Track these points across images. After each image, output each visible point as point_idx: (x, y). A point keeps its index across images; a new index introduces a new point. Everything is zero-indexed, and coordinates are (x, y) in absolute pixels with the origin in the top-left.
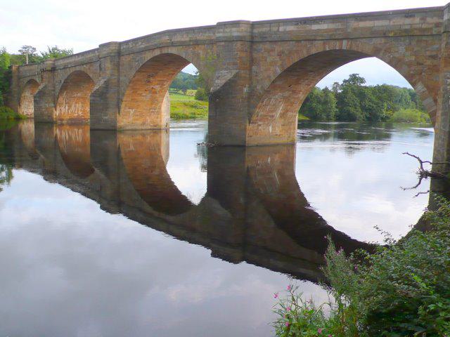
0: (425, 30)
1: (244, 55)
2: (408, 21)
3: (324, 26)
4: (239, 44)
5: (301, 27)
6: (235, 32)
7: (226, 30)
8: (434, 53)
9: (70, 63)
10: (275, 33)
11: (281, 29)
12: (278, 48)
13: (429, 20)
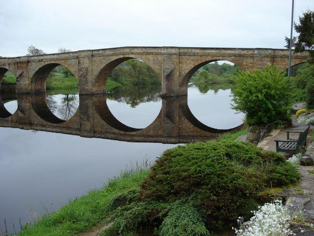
1: (177, 60)
2: (243, 52)
3: (213, 51)
4: (175, 56)
6: (173, 51)
9: (47, 59)
10: (190, 52)
11: (193, 51)
12: (191, 58)
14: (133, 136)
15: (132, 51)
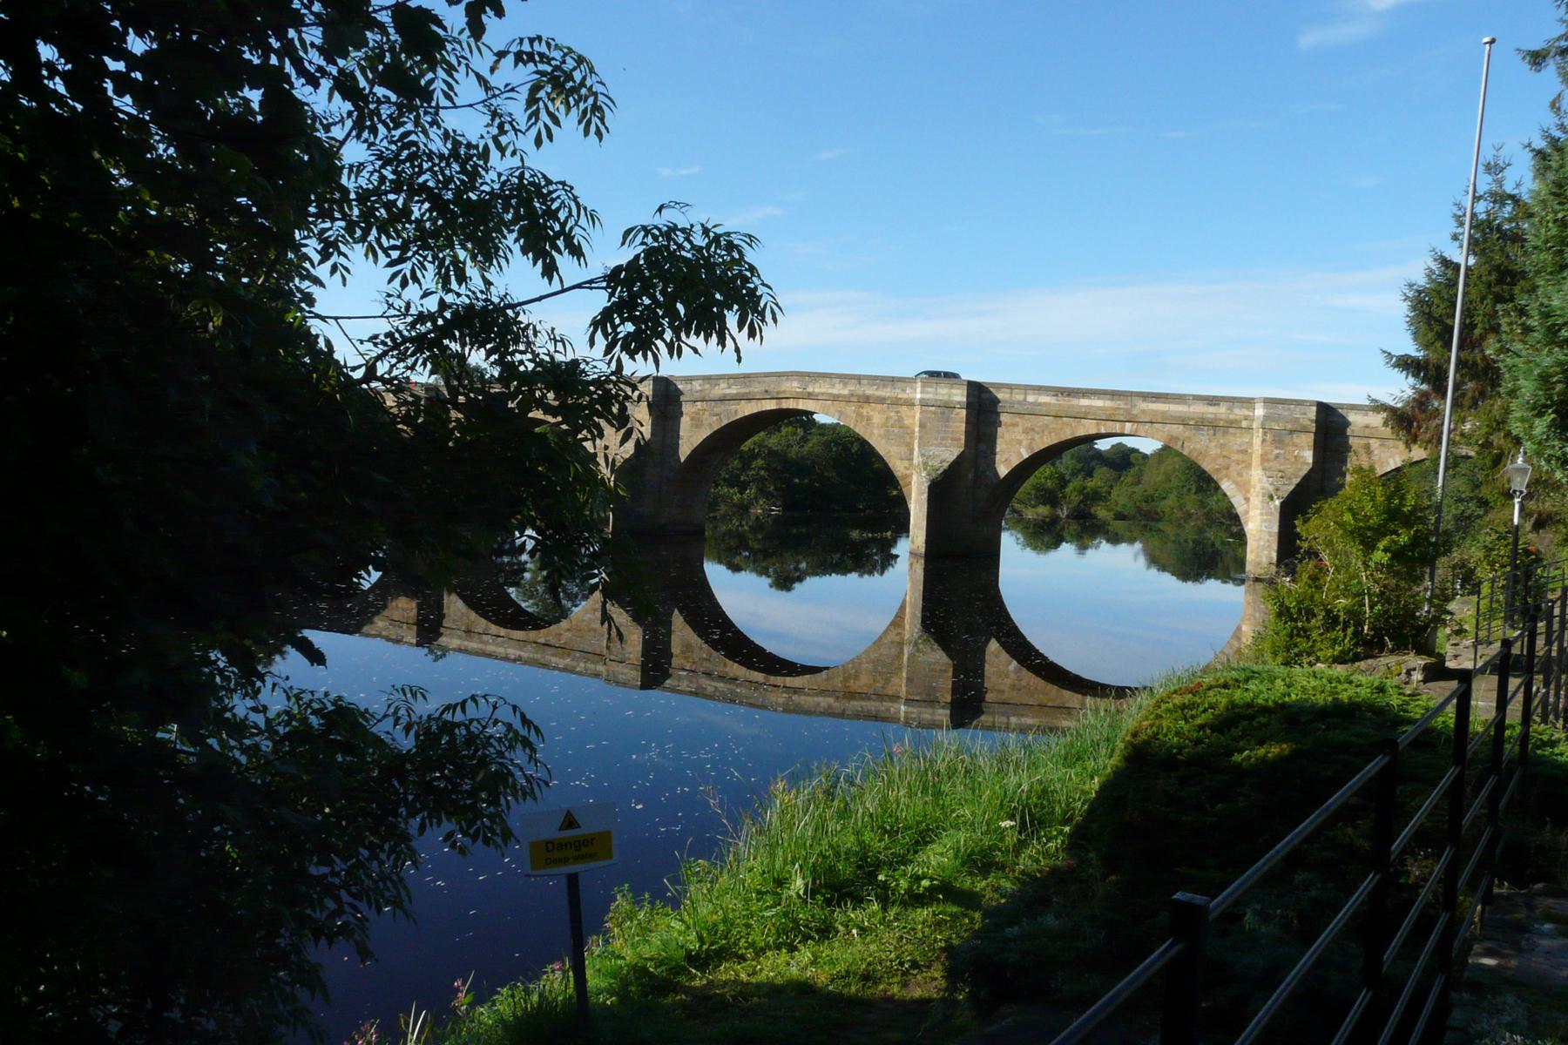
0: (1232, 422)
5: (1064, 401)
7: (940, 390)
8: (1243, 448)
11: (1030, 398)
13: (1237, 411)
14: (796, 691)
15: (810, 389)
